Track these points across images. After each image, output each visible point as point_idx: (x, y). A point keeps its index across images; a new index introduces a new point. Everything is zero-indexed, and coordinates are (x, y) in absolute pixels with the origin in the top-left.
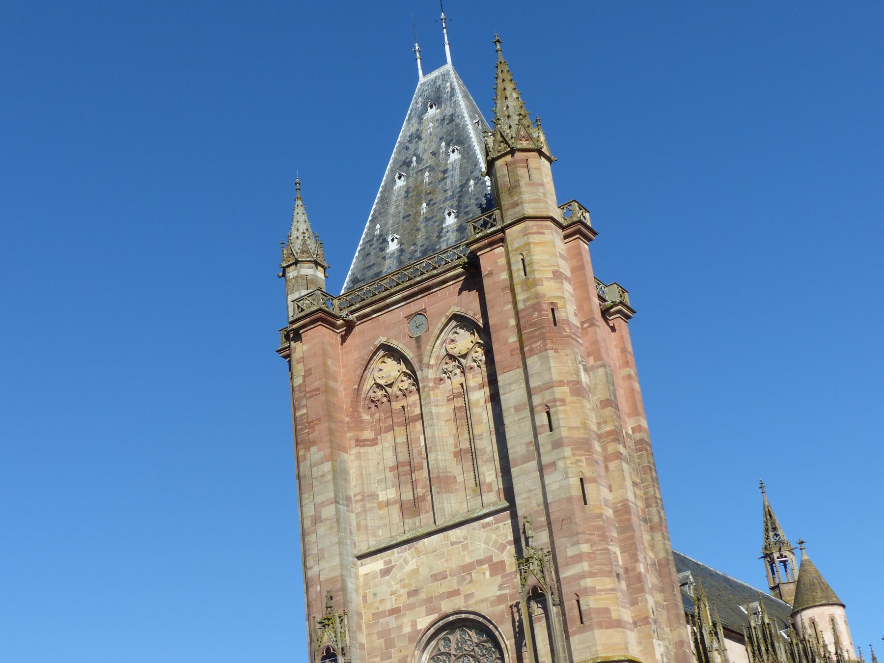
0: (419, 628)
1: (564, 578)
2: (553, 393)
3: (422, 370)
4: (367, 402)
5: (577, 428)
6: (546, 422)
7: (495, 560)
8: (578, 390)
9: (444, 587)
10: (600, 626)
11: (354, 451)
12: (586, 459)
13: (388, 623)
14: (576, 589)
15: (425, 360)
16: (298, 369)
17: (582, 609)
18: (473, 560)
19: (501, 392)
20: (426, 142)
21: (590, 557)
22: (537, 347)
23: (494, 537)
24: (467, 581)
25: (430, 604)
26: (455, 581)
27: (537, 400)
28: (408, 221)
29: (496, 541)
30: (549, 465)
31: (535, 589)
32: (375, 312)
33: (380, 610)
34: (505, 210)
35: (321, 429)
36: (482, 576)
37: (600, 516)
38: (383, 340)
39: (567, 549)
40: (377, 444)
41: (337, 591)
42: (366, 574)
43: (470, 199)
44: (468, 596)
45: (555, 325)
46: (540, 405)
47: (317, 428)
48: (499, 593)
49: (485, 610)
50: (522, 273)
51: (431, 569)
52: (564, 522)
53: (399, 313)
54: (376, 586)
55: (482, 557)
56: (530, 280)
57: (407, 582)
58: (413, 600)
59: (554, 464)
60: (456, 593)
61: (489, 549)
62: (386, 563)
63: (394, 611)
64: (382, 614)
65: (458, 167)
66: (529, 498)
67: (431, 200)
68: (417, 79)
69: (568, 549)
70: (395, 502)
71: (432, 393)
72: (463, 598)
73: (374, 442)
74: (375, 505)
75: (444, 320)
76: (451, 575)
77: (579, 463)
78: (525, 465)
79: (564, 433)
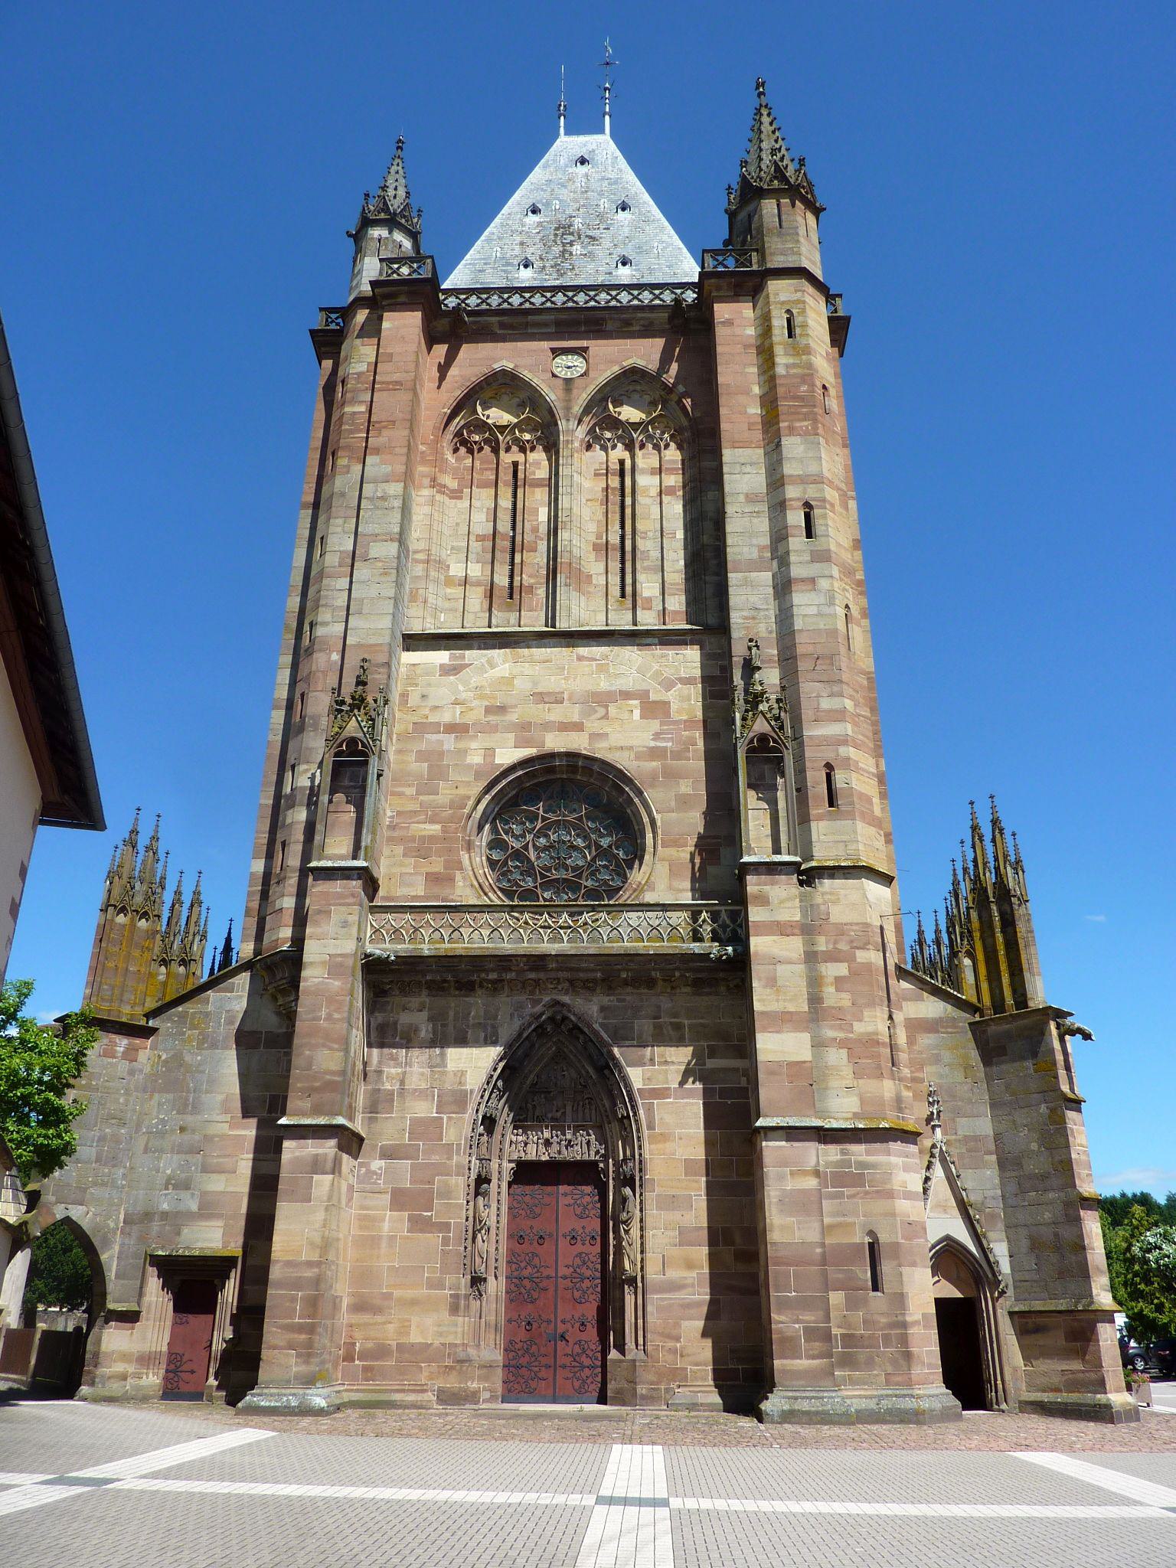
1: (811, 737)
3: (568, 420)
7: (653, 697)
9: (556, 714)
11: (426, 492)
13: (441, 743)
14: (829, 755)
16: (362, 352)
18: (613, 689)
19: (725, 469)
22: (801, 427)
23: (656, 667)
24: (598, 715)
27: (792, 492)
29: (658, 673)
30: (803, 580)
31: (763, 738)
33: (431, 719)
34: (771, 254)
35: (398, 435)
36: (626, 716)
40: (461, 498)
41: (378, 665)
42: (414, 665)
44: (595, 737)
47: (385, 432)
48: (652, 744)
49: (623, 761)
51: (535, 684)
52: (819, 662)
54: (429, 685)
59: (812, 581)
60: (578, 727)
61: (644, 680)
63: (456, 729)
64: (435, 728)
66: (754, 618)
68: (557, 135)
70: (478, 584)
71: (576, 455)
73: (456, 495)
78: (754, 575)
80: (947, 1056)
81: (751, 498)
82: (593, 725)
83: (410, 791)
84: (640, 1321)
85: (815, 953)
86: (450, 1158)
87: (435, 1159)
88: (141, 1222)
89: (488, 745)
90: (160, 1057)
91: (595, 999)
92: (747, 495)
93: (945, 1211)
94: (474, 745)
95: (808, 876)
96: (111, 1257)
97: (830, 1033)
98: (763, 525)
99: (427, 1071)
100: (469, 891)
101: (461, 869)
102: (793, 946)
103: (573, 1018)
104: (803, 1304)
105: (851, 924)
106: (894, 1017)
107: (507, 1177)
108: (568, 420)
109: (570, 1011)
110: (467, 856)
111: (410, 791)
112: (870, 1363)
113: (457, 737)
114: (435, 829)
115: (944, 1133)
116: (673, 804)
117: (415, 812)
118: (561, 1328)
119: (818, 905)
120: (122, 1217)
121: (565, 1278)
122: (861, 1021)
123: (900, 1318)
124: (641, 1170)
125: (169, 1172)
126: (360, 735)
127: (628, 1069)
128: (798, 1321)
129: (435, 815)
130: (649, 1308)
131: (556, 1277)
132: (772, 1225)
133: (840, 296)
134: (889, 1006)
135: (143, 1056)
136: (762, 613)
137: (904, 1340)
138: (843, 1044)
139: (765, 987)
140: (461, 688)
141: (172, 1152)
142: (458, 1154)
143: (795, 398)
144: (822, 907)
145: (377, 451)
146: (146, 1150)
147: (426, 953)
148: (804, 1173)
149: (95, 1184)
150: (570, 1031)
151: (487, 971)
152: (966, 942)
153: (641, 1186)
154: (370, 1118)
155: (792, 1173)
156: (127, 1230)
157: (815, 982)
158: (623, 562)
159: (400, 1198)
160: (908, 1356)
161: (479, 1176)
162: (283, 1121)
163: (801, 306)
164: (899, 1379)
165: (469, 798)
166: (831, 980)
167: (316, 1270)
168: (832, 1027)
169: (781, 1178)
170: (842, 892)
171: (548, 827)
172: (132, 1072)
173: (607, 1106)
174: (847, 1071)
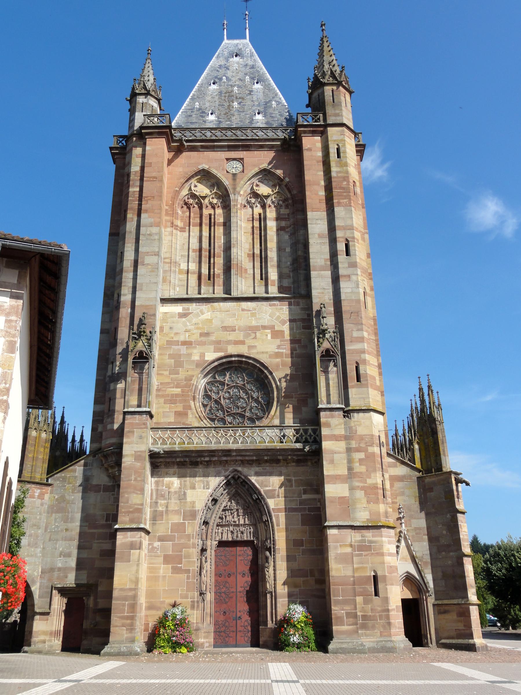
0: (206, 359)
1: (349, 350)
3: (235, 195)
4: (182, 203)
7: (276, 328)
9: (232, 336)
11: (169, 229)
13: (179, 350)
14: (357, 359)
15: (238, 189)
19: (309, 222)
22: (343, 202)
23: (278, 314)
25: (218, 345)
26: (242, 335)
27: (339, 234)
29: (279, 317)
30: (345, 276)
31: (328, 351)
32: (202, 147)
33: (175, 339)
36: (265, 337)
38: (206, 167)
39: (353, 332)
40: (185, 231)
42: (166, 313)
44: (250, 347)
46: (342, 237)
47: (149, 202)
48: (277, 351)
51: (222, 322)
52: (352, 314)
53: (223, 155)
54: (173, 322)
55: (266, 324)
57: (200, 326)
58: (203, 339)
59: (349, 276)
61: (272, 320)
62: (184, 309)
64: (177, 343)
66: (323, 293)
70: (194, 273)
71: (239, 211)
72: (247, 348)
73: (182, 230)
74: (177, 270)
75: (257, 170)
76: (239, 330)
78: (323, 272)
80: (407, 492)
81: (320, 236)
82: (249, 342)
84: (274, 611)
85: (351, 448)
86: (189, 540)
87: (182, 541)
88: (49, 572)
89: (202, 351)
90: (54, 497)
91: (253, 469)
92: (319, 235)
93: (406, 561)
94: (195, 351)
95: (347, 413)
96: (36, 589)
97: (357, 484)
98: (326, 249)
99: (178, 502)
100: (194, 420)
101: (191, 409)
102: (341, 445)
103: (243, 477)
104: (345, 602)
105: (366, 435)
107: (214, 548)
108: (235, 195)
109: (241, 474)
110: (193, 403)
111: (167, 373)
112: (373, 627)
113: (187, 347)
114: (178, 391)
115: (406, 526)
117: (169, 383)
118: (239, 614)
119: (352, 427)
120: (40, 570)
121: (240, 592)
122: (370, 478)
123: (386, 608)
124: (274, 544)
125: (61, 549)
126: (144, 349)
127: (268, 500)
128: (343, 610)
129: (178, 384)
130: (278, 605)
131: (236, 592)
132: (332, 568)
133: (361, 133)
134: (382, 472)
135: (47, 497)
136: (326, 291)
137: (388, 617)
138: (362, 488)
139: (329, 463)
140: (188, 324)
141: (62, 540)
142: (193, 538)
143: (341, 188)
144: (354, 428)
145: (146, 211)
146: (50, 540)
147: (177, 449)
148: (346, 546)
149: (28, 556)
150: (241, 483)
151: (204, 457)
152: (416, 438)
153: (274, 551)
154: (153, 523)
155: (341, 546)
156: (43, 576)
157: (350, 461)
158: (261, 263)
159: (167, 559)
160: (389, 624)
161: (202, 548)
162: (116, 527)
163: (343, 142)
164: (386, 634)
166: (357, 460)
167: (134, 592)
169: (336, 548)
170: (363, 421)
171: (230, 388)
172: (42, 505)
173: (258, 515)
174: (364, 501)
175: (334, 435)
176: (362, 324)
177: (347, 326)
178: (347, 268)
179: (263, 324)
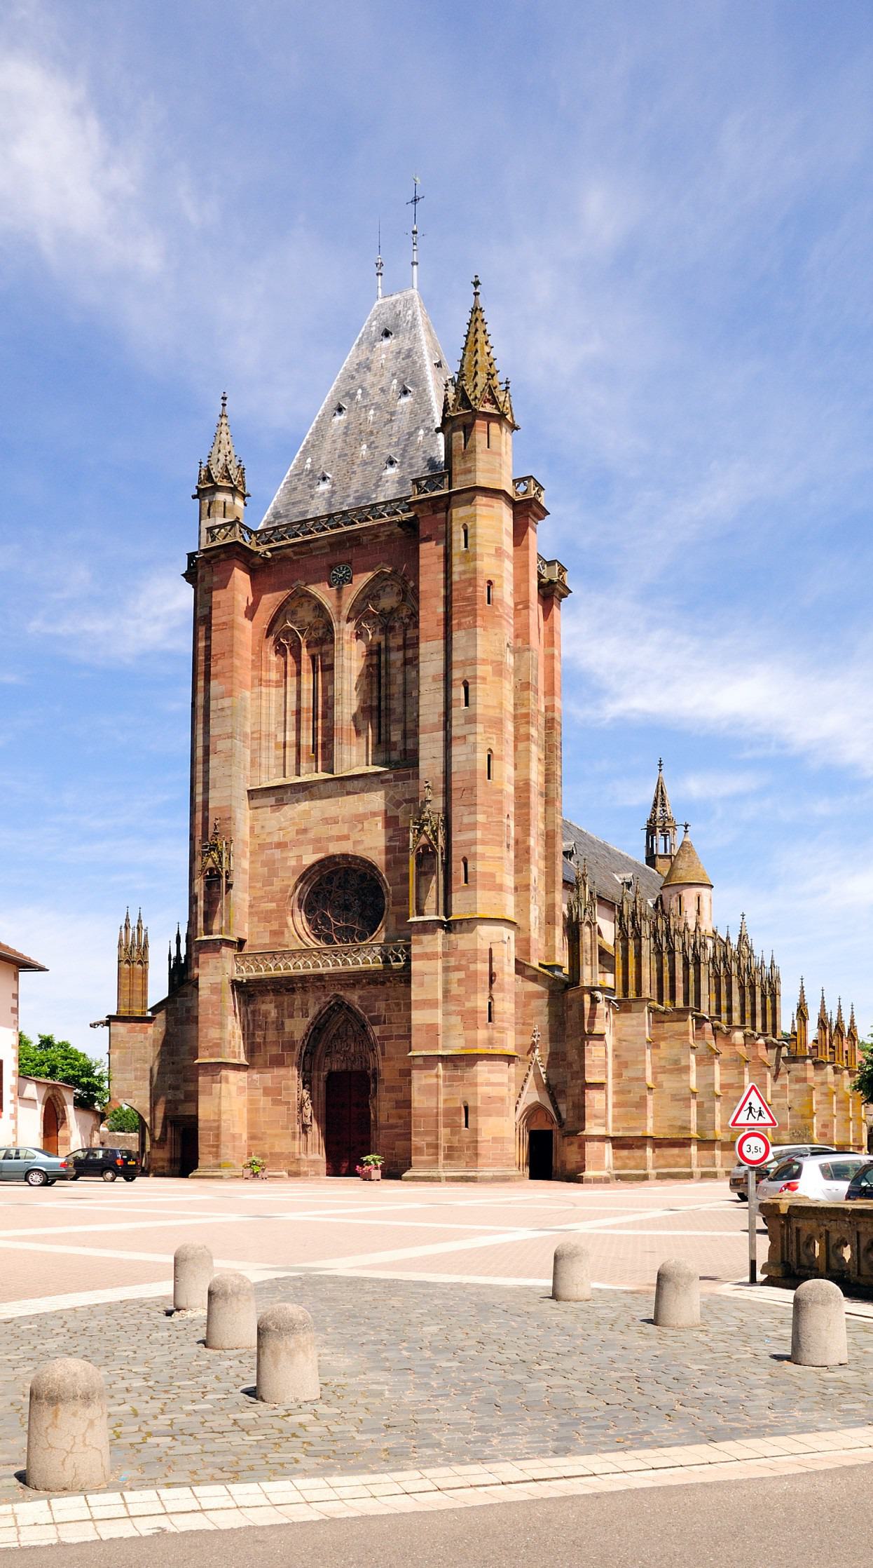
0: (304, 863)
2: (476, 670)
5: (494, 707)
6: (463, 697)
8: (499, 670)
9: (335, 830)
10: (484, 887)
12: (497, 738)
13: (273, 854)
14: (465, 852)
17: (469, 871)
20: (376, 375)
21: (486, 827)
27: (457, 674)
28: (344, 460)
33: (268, 840)
37: (501, 791)
43: (417, 450)
44: (356, 843)
45: (489, 603)
50: (463, 544)
56: (471, 554)
60: (346, 838)
63: (281, 845)
65: (408, 411)
67: (373, 442)
69: (464, 817)
77: (490, 741)
79: (480, 710)
82: (355, 836)
83: (259, 885)
85: (449, 967)
94: (291, 854)
98: (440, 698)
104: (426, 1133)
106: (494, 997)
112: (459, 1158)
116: (399, 880)
129: (273, 897)
137: (476, 1148)
144: (455, 942)
155: (425, 1077)
157: (446, 982)
160: (477, 1155)
165: (289, 886)
166: (456, 980)
168: (455, 1005)
169: (420, 1079)
175: (426, 953)
176: (476, 804)
177: (456, 810)
178: (462, 725)
179: (373, 810)
